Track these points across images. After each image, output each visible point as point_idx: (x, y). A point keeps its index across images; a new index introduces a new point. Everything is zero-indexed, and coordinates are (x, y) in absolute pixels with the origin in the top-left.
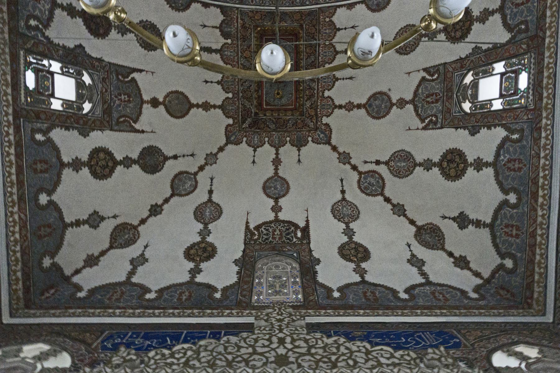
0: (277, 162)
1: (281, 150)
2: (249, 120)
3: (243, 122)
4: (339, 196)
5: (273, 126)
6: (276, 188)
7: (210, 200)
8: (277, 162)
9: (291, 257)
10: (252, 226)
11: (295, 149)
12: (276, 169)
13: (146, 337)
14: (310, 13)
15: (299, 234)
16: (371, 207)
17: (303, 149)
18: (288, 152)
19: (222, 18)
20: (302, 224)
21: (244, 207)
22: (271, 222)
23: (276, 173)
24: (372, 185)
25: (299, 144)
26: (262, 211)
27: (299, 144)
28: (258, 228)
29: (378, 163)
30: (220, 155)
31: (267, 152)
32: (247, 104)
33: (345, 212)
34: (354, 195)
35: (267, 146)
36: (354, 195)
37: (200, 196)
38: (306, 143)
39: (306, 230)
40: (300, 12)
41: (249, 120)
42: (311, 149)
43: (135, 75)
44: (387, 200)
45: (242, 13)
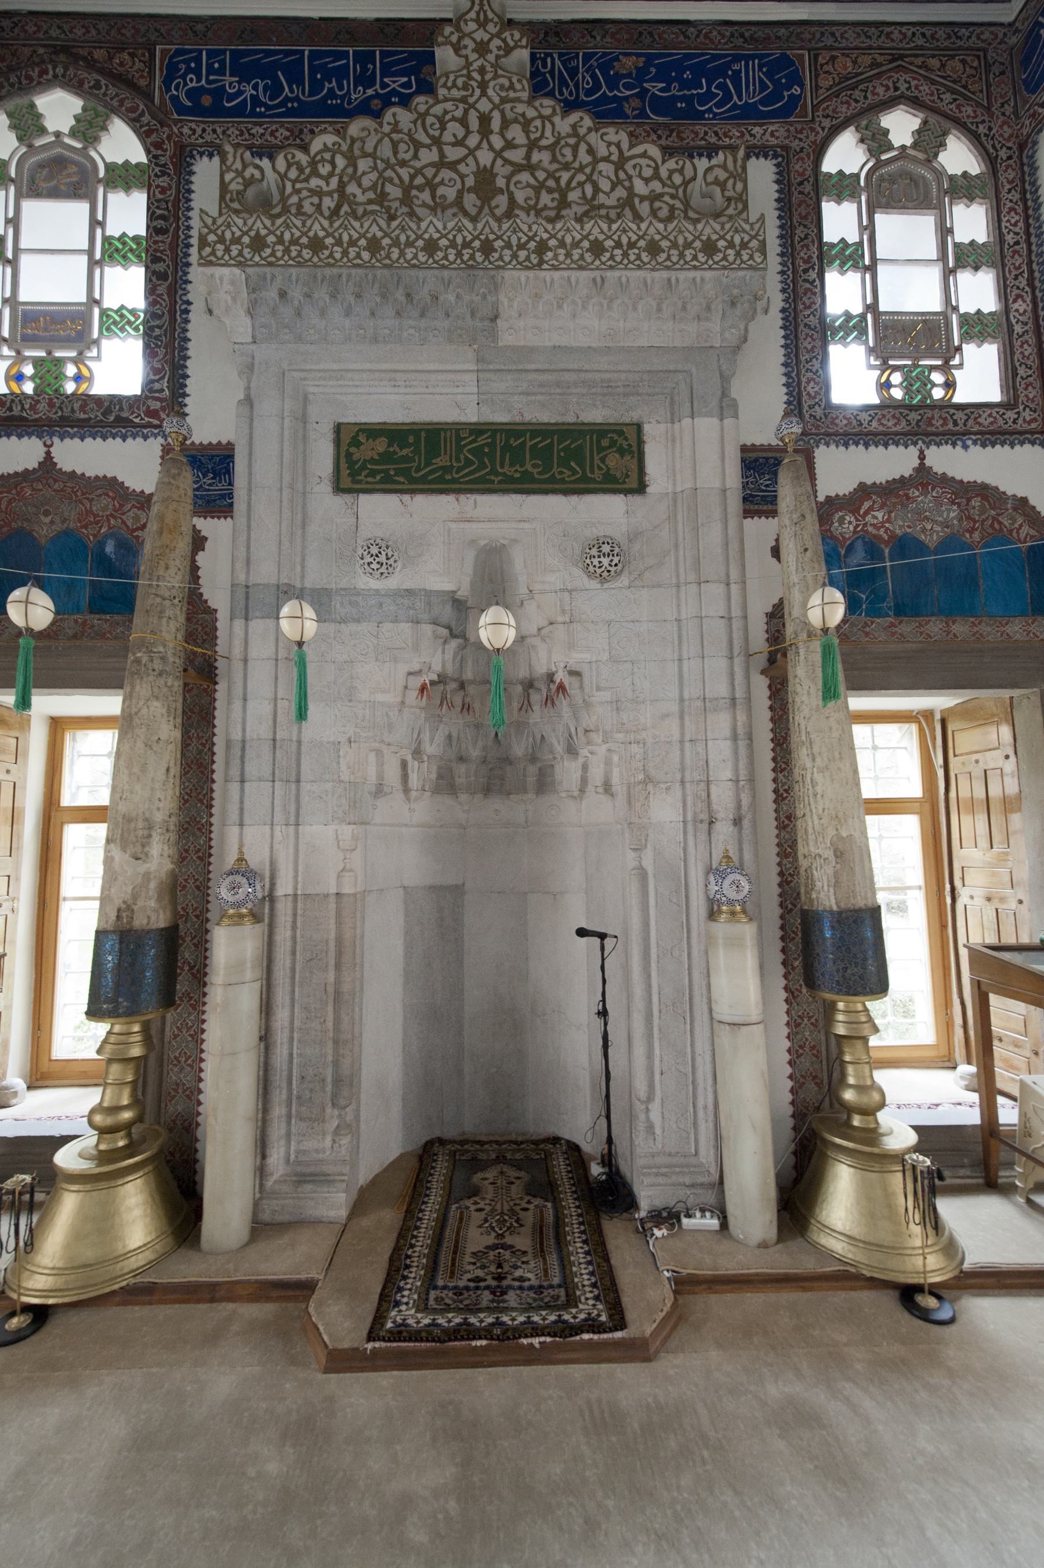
13: (244, 72)
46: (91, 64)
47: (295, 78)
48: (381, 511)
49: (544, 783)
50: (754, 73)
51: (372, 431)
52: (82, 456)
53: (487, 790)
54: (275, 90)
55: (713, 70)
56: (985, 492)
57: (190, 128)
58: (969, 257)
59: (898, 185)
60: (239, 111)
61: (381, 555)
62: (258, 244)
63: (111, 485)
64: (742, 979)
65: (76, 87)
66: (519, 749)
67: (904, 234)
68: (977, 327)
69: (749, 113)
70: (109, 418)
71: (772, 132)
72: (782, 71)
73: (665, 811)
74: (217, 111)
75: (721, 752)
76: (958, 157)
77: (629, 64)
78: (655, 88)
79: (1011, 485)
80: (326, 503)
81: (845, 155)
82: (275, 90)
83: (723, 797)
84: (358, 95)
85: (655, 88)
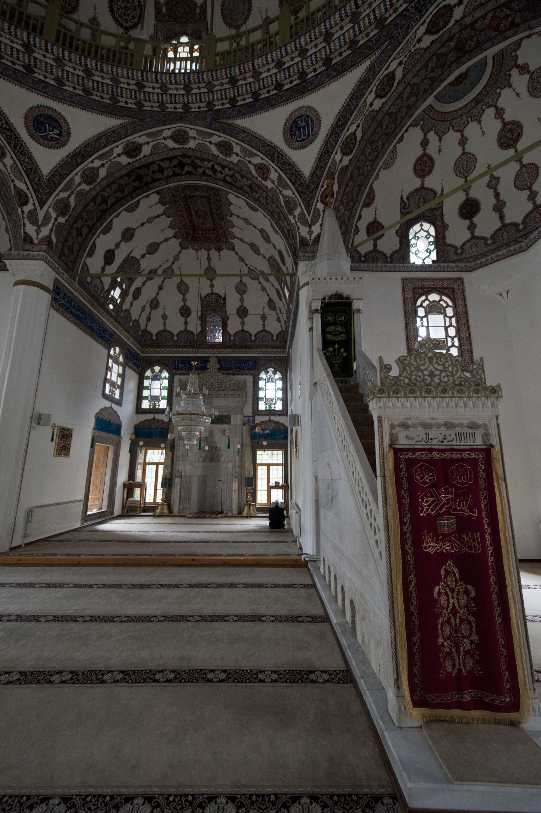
1: (210, 252)
2: (190, 237)
3: (187, 238)
5: (204, 240)
8: (209, 259)
10: (203, 297)
11: (217, 252)
12: (209, 263)
13: (182, 363)
14: (213, 188)
15: (222, 302)
16: (252, 285)
17: (222, 252)
18: (213, 253)
19: (159, 196)
20: (223, 296)
22: (210, 294)
23: (209, 265)
25: (219, 249)
26: (206, 291)
27: (219, 249)
28: (205, 297)
30: (180, 255)
32: (187, 231)
33: (241, 289)
34: (246, 280)
38: (222, 249)
39: (224, 299)
40: (206, 186)
41: (190, 237)
42: (225, 252)
43: (131, 255)
45: (169, 189)
46: (161, 363)
49: (219, 461)
50: (251, 363)
52: (158, 417)
53: (211, 461)
55: (246, 362)
56: (278, 422)
57: (174, 371)
63: (162, 421)
65: (159, 366)
66: (215, 456)
69: (250, 369)
70: (163, 411)
72: (255, 363)
73: (230, 465)
78: (237, 365)
79: (281, 422)
83: (237, 464)
85: (237, 365)
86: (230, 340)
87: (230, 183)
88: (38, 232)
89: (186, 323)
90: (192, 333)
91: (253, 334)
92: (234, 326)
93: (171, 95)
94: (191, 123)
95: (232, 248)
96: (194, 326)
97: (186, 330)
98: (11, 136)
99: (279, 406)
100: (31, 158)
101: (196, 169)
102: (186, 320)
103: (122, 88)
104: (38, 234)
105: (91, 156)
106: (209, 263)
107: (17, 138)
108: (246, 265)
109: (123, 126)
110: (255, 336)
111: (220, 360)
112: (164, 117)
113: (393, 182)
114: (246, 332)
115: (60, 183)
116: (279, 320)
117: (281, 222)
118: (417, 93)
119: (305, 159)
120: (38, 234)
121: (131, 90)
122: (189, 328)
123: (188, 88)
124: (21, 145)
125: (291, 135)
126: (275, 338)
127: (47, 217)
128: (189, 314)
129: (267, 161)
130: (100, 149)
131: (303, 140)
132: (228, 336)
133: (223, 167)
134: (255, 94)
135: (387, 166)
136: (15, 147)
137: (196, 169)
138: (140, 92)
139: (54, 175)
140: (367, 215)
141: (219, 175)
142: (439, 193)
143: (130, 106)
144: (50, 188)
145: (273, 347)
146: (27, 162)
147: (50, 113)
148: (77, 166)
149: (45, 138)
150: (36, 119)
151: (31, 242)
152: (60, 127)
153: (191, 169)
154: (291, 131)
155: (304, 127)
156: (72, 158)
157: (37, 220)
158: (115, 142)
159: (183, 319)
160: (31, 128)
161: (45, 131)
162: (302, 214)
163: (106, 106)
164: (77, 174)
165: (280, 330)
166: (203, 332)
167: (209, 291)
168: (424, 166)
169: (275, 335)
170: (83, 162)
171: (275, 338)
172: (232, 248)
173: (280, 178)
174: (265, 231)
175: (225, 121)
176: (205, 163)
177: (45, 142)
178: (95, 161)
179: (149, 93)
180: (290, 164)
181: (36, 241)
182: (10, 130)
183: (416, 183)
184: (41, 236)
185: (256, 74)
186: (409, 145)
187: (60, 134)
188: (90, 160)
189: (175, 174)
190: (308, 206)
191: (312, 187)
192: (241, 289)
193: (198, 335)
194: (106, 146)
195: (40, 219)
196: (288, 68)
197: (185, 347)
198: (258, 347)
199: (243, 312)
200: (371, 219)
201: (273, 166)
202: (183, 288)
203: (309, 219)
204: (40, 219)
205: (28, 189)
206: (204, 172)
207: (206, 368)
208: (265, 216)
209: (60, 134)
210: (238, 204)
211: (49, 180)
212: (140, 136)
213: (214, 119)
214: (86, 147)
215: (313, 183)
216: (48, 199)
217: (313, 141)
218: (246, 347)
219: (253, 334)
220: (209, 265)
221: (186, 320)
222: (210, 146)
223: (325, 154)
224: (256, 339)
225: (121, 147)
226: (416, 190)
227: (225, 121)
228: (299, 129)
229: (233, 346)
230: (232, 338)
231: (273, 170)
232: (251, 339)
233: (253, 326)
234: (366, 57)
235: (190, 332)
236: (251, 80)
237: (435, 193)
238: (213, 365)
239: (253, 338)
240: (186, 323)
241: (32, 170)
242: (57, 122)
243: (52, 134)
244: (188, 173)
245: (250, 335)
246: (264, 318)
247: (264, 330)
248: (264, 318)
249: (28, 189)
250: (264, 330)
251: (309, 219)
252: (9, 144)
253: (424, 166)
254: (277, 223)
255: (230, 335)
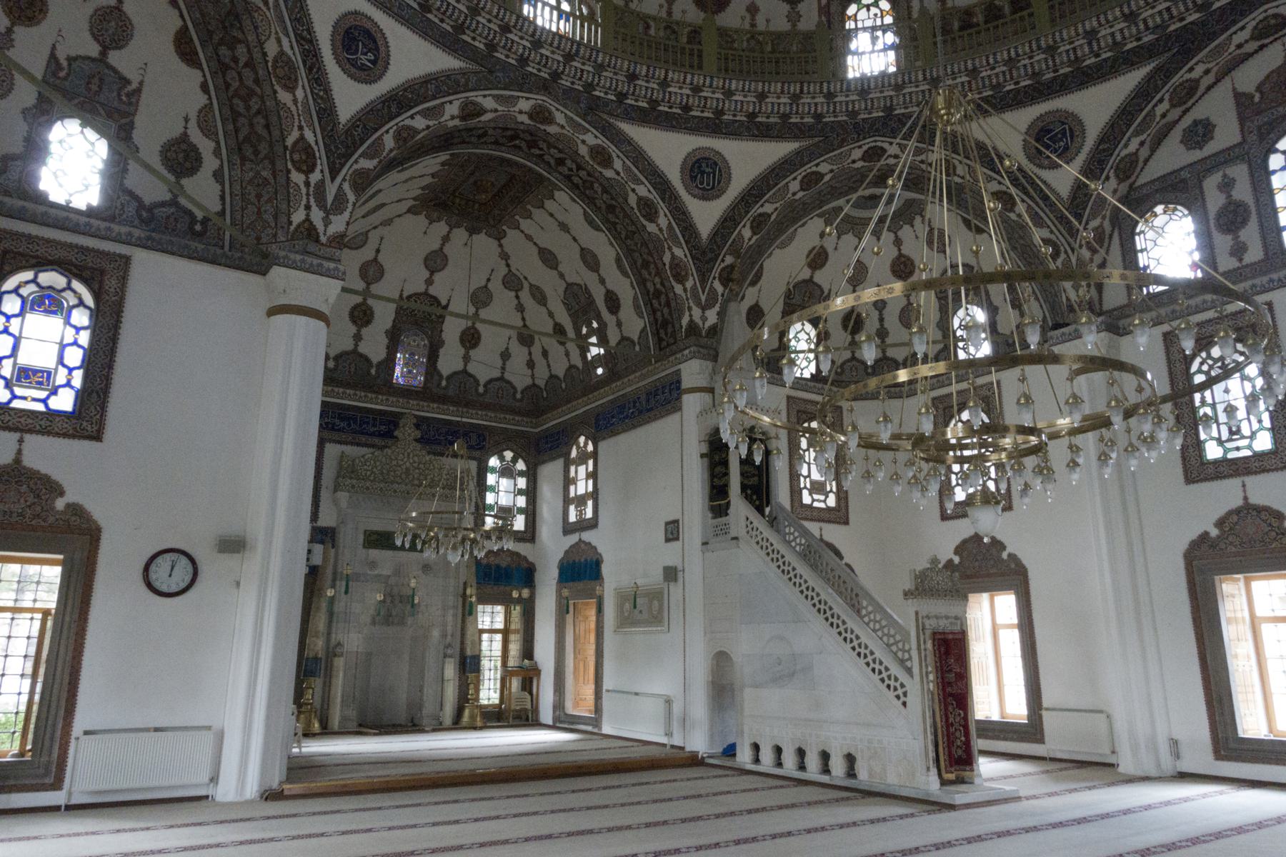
0: (446, 239)
1: (455, 230)
4: (483, 283)
6: (436, 261)
7: (375, 260)
8: (446, 239)
9: (426, 334)
12: (443, 245)
13: (342, 419)
14: (541, 175)
18: (460, 235)
20: (444, 302)
21: (403, 274)
23: (441, 249)
24: (512, 282)
25: (472, 231)
27: (472, 231)
28: (409, 297)
29: (526, 278)
31: (441, 228)
34: (496, 286)
35: (443, 223)
36: (496, 286)
37: (367, 253)
44: (517, 297)
47: (355, 422)
48: (375, 553)
50: (474, 436)
51: (376, 533)
54: (349, 425)
56: (518, 554)
58: (520, 492)
59: (506, 472)
60: (339, 430)
61: (373, 565)
62: (353, 487)
64: (450, 671)
67: (505, 483)
68: (521, 511)
71: (477, 454)
72: (481, 437)
73: (436, 633)
74: (333, 429)
75: (450, 618)
76: (521, 465)
77: (444, 430)
79: (523, 553)
80: (362, 552)
81: (494, 462)
82: (349, 425)
83: (449, 628)
84: (372, 430)
86: (439, 384)
87: (577, 186)
88: (327, 223)
89: (358, 338)
90: (367, 360)
91: (482, 382)
92: (449, 361)
93: (542, 55)
94: (557, 101)
95: (499, 237)
96: (374, 346)
97: (355, 351)
98: (309, 51)
99: (519, 523)
100: (327, 90)
101: (530, 147)
102: (359, 331)
103: (478, 22)
104: (326, 226)
105: (411, 108)
106: (443, 245)
107: (315, 56)
108: (508, 265)
109: (463, 73)
110: (485, 386)
111: (420, 423)
112: (524, 83)
113: (785, 265)
114: (471, 375)
115: (363, 141)
116: (531, 364)
117: (644, 272)
118: (835, 192)
119: (706, 215)
120: (326, 226)
121: (490, 29)
122: (363, 349)
123: (569, 57)
124: (319, 69)
125: (691, 177)
126: (519, 396)
127: (340, 198)
128: (368, 322)
129: (654, 196)
130: (426, 100)
131: (704, 189)
132: (436, 377)
133: (579, 168)
134: (654, 103)
135: (783, 246)
136: (310, 69)
137: (530, 147)
138: (501, 35)
139: (355, 126)
140: (751, 296)
141: (565, 170)
142: (826, 292)
143: (477, 44)
144: (347, 147)
145: (513, 411)
146: (321, 98)
147: (368, 25)
148: (391, 119)
149: (353, 63)
150: (347, 32)
151: (317, 240)
152: (377, 49)
153: (523, 145)
154: (691, 170)
155: (708, 174)
156: (383, 102)
157: (325, 201)
158: (450, 94)
159: (353, 329)
160: (339, 44)
161: (356, 52)
162: (694, 288)
163: (444, 34)
164: (387, 132)
165: (529, 381)
166: (389, 362)
167: (422, 289)
168: (818, 259)
169: (519, 390)
170: (399, 115)
171: (519, 396)
172: (499, 237)
173: (670, 226)
174: (595, 256)
175: (605, 116)
176: (552, 151)
177: (353, 70)
178: (418, 117)
179: (513, 41)
180: (684, 213)
181: (323, 239)
182: (310, 42)
183: (806, 274)
184: (332, 230)
185: (664, 84)
186: (809, 233)
187: (374, 62)
188: (409, 114)
189: (496, 143)
190: (703, 281)
191: (710, 255)
192: (481, 298)
193: (379, 364)
194: (435, 98)
195: (330, 199)
196: (706, 98)
197: (347, 385)
198: (486, 407)
199: (470, 339)
200: (753, 302)
201: (662, 208)
202: (372, 271)
203: (703, 298)
204: (330, 199)
205: (317, 143)
206: (541, 156)
207: (389, 435)
208: (611, 244)
209: (374, 62)
210: (565, 205)
211: (346, 132)
212: (485, 96)
213: (590, 108)
214: (405, 90)
215: (712, 250)
216: (343, 165)
217: (718, 197)
218: (468, 404)
219: (482, 382)
220: (441, 249)
221: (359, 331)
222: (631, 194)
223: (729, 222)
224: (486, 391)
225: (457, 104)
226: (804, 281)
227: (605, 116)
228: (703, 173)
229: (443, 399)
230: (444, 383)
231: (662, 214)
232: (477, 390)
233: (484, 366)
234: (796, 138)
235: (361, 355)
236: (655, 86)
237: (823, 292)
238: (407, 432)
239: (481, 390)
240: (358, 338)
241: (326, 112)
242: (375, 42)
243: (365, 59)
244: (515, 146)
245: (477, 381)
246: (505, 355)
247: (501, 379)
248: (505, 355)
249: (317, 143)
250: (501, 379)
251: (703, 298)
252: (304, 62)
253: (818, 259)
254: (633, 264)
255: (441, 376)
